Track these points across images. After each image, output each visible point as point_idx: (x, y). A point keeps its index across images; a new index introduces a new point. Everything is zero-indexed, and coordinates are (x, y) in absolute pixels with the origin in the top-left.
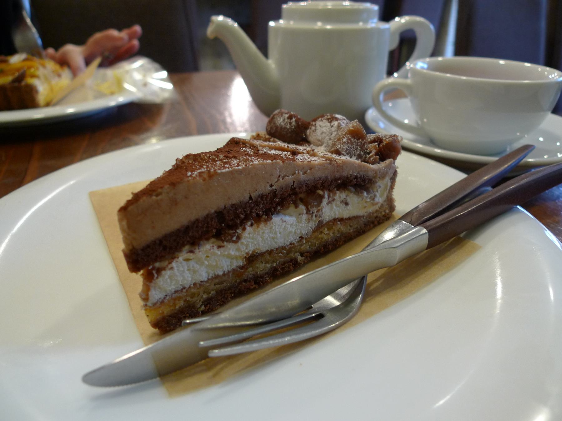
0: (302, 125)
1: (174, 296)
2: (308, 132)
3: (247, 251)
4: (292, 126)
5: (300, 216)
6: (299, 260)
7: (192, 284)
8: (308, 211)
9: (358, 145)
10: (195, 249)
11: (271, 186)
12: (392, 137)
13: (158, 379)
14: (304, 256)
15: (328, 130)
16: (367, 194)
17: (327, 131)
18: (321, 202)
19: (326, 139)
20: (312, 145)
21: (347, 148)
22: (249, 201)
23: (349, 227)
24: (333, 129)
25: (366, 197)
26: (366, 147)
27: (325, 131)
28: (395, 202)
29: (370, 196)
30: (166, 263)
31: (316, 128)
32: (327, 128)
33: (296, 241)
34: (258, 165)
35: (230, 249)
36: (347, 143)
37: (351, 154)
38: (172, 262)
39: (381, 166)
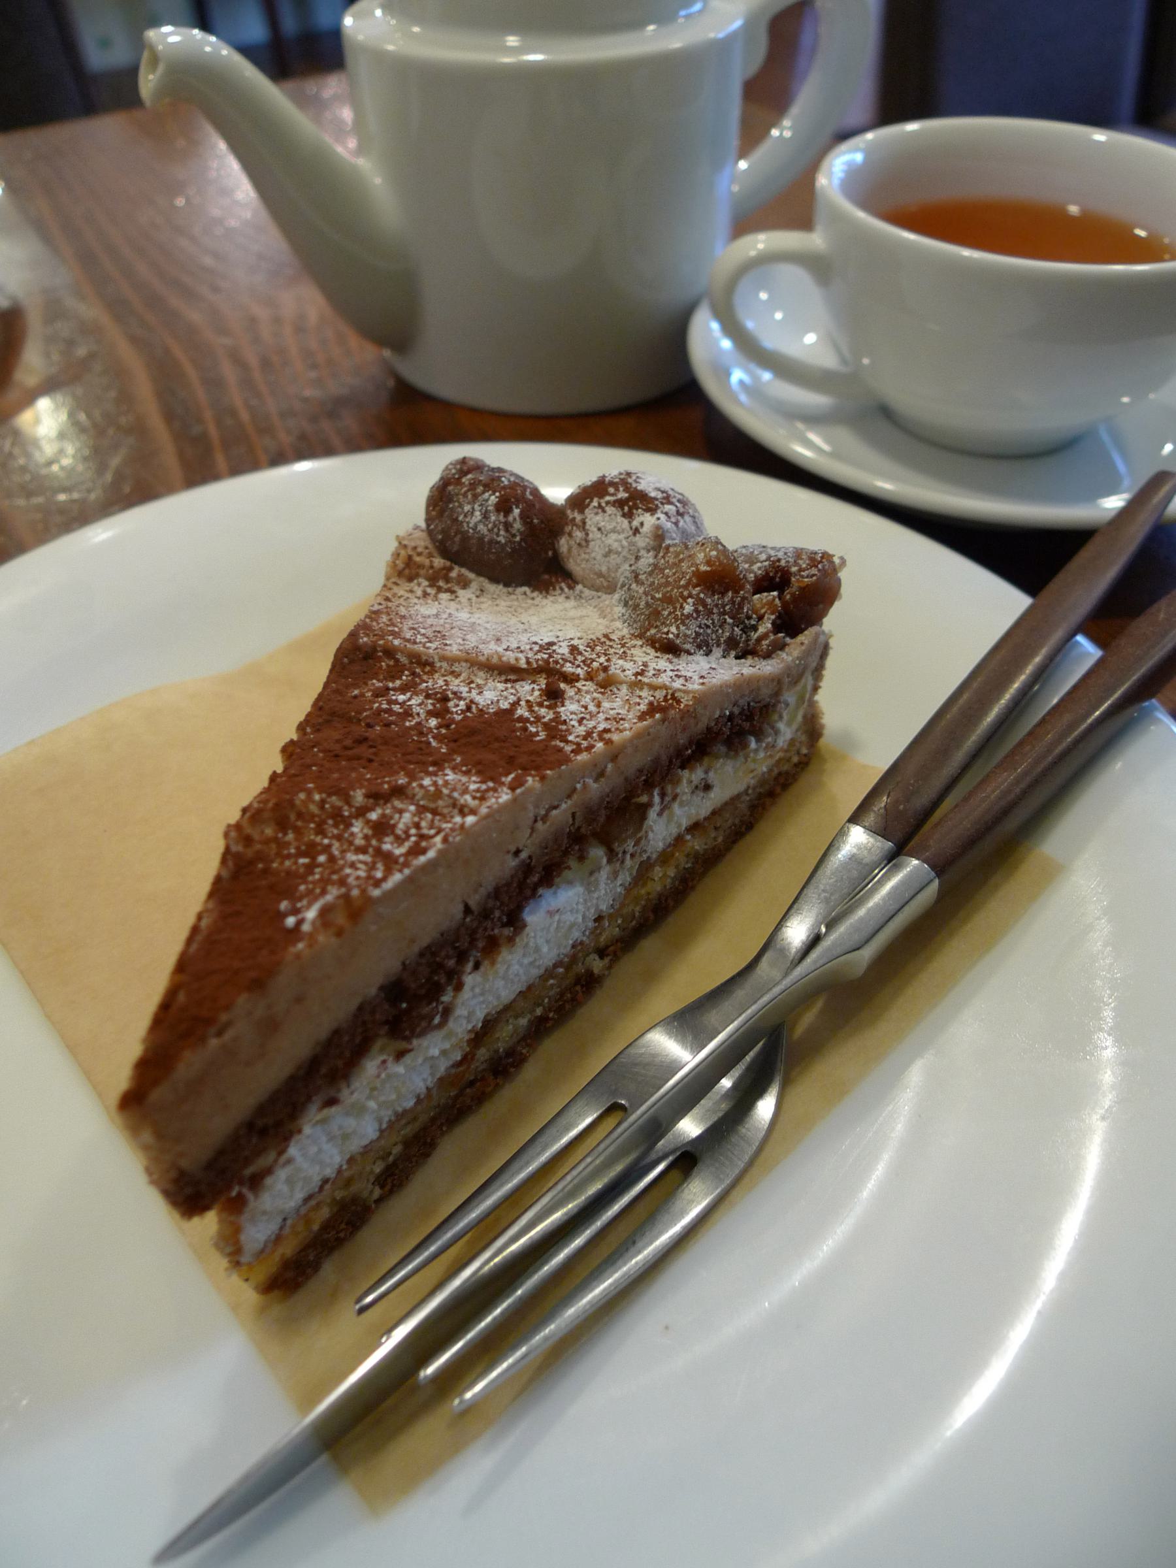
0: (543, 526)
1: (303, 1211)
2: (563, 544)
3: (470, 1027)
4: (514, 536)
5: (593, 879)
6: (596, 971)
7: (344, 1162)
8: (612, 855)
9: (724, 613)
10: (339, 1090)
11: (517, 852)
12: (817, 567)
13: (324, 1458)
14: (608, 955)
15: (625, 543)
16: (758, 741)
17: (623, 547)
18: (643, 817)
19: (620, 570)
20: (579, 587)
21: (697, 629)
22: (465, 919)
23: (713, 835)
24: (641, 541)
25: (756, 751)
26: (747, 612)
27: (615, 545)
28: (821, 718)
29: (764, 745)
30: (272, 1155)
31: (587, 534)
32: (622, 536)
33: (587, 933)
34: (477, 823)
35: (428, 1048)
36: (695, 615)
37: (707, 645)
38: (287, 1147)
39: (790, 658)
